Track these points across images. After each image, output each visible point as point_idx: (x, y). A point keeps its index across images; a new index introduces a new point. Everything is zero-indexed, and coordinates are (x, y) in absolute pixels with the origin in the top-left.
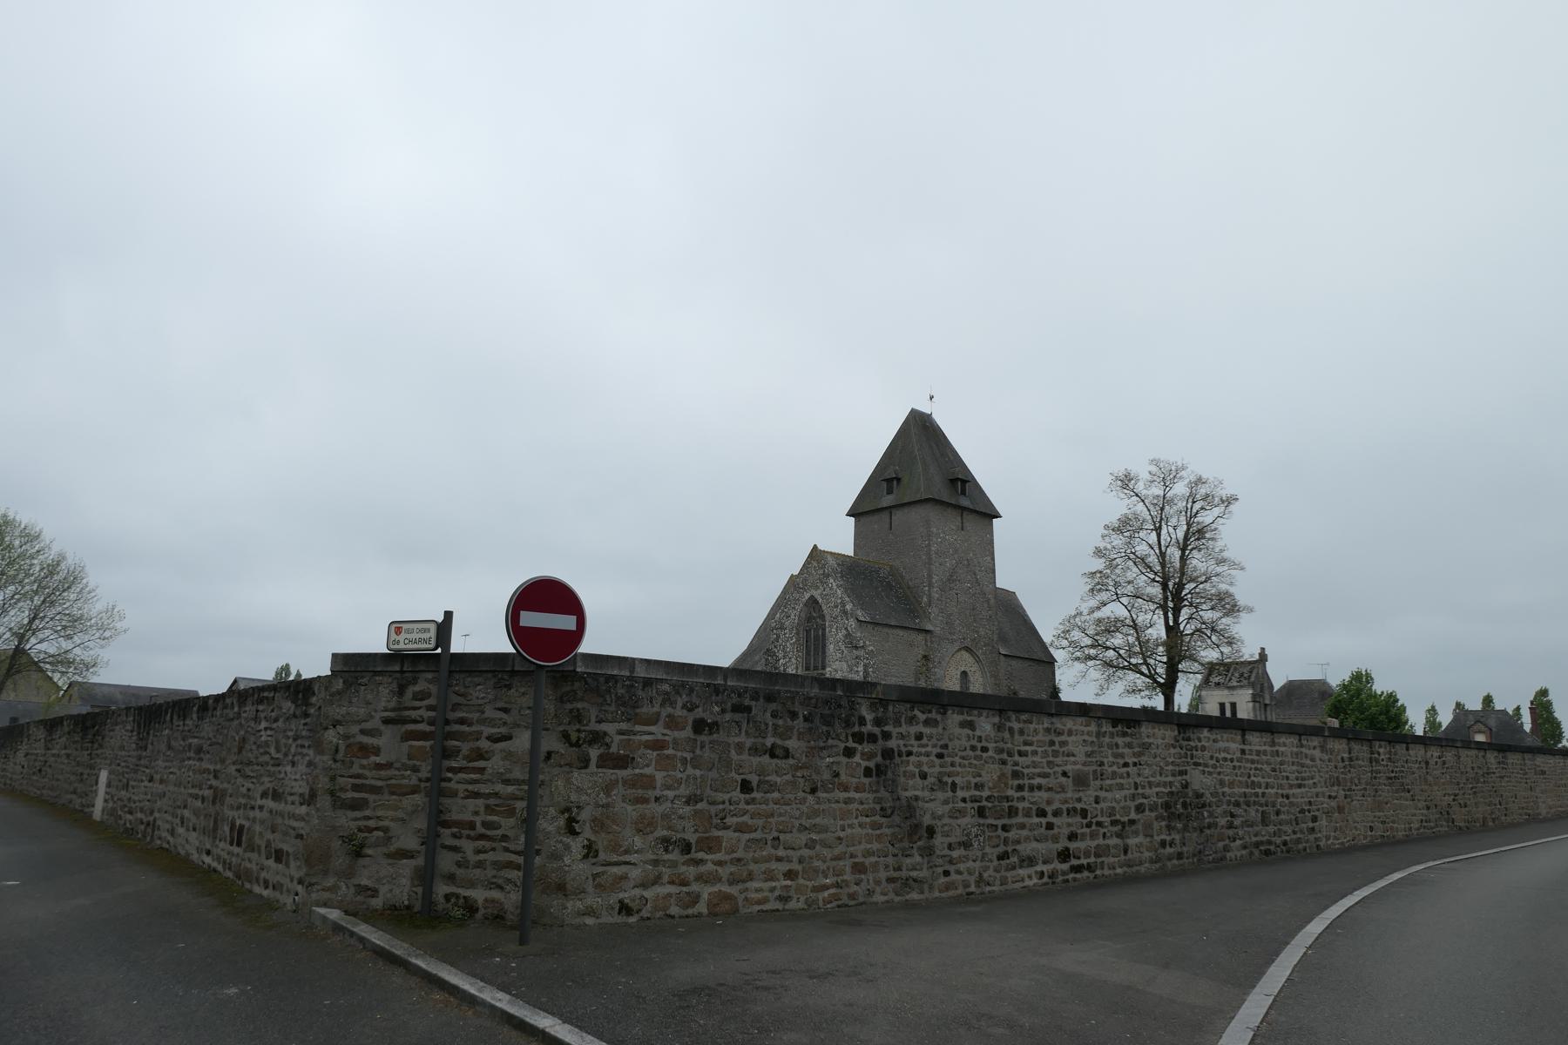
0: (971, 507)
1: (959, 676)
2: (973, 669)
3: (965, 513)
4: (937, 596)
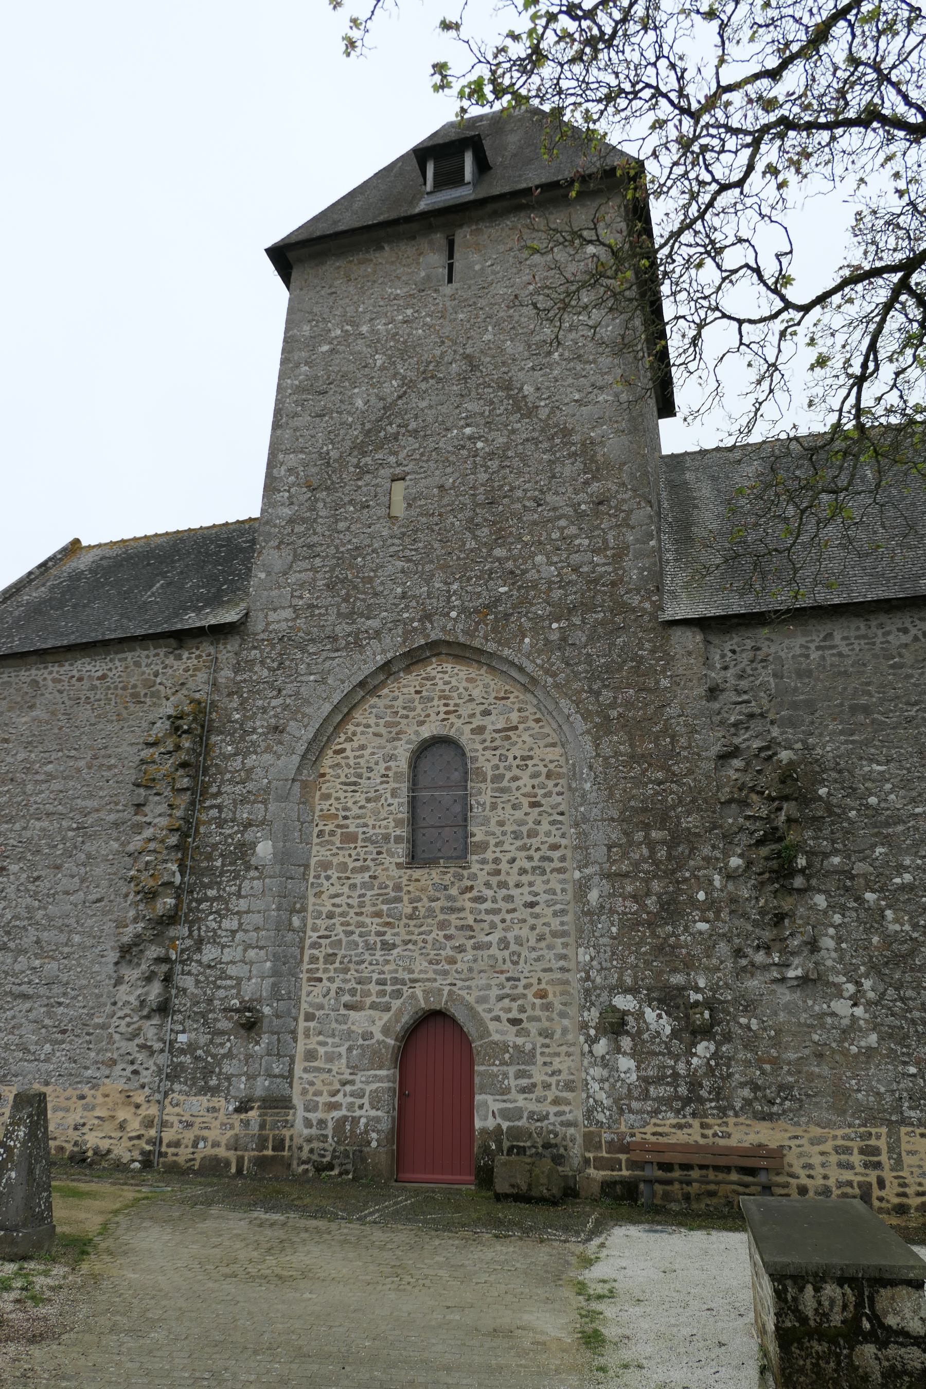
1: (402, 764)
2: (495, 722)
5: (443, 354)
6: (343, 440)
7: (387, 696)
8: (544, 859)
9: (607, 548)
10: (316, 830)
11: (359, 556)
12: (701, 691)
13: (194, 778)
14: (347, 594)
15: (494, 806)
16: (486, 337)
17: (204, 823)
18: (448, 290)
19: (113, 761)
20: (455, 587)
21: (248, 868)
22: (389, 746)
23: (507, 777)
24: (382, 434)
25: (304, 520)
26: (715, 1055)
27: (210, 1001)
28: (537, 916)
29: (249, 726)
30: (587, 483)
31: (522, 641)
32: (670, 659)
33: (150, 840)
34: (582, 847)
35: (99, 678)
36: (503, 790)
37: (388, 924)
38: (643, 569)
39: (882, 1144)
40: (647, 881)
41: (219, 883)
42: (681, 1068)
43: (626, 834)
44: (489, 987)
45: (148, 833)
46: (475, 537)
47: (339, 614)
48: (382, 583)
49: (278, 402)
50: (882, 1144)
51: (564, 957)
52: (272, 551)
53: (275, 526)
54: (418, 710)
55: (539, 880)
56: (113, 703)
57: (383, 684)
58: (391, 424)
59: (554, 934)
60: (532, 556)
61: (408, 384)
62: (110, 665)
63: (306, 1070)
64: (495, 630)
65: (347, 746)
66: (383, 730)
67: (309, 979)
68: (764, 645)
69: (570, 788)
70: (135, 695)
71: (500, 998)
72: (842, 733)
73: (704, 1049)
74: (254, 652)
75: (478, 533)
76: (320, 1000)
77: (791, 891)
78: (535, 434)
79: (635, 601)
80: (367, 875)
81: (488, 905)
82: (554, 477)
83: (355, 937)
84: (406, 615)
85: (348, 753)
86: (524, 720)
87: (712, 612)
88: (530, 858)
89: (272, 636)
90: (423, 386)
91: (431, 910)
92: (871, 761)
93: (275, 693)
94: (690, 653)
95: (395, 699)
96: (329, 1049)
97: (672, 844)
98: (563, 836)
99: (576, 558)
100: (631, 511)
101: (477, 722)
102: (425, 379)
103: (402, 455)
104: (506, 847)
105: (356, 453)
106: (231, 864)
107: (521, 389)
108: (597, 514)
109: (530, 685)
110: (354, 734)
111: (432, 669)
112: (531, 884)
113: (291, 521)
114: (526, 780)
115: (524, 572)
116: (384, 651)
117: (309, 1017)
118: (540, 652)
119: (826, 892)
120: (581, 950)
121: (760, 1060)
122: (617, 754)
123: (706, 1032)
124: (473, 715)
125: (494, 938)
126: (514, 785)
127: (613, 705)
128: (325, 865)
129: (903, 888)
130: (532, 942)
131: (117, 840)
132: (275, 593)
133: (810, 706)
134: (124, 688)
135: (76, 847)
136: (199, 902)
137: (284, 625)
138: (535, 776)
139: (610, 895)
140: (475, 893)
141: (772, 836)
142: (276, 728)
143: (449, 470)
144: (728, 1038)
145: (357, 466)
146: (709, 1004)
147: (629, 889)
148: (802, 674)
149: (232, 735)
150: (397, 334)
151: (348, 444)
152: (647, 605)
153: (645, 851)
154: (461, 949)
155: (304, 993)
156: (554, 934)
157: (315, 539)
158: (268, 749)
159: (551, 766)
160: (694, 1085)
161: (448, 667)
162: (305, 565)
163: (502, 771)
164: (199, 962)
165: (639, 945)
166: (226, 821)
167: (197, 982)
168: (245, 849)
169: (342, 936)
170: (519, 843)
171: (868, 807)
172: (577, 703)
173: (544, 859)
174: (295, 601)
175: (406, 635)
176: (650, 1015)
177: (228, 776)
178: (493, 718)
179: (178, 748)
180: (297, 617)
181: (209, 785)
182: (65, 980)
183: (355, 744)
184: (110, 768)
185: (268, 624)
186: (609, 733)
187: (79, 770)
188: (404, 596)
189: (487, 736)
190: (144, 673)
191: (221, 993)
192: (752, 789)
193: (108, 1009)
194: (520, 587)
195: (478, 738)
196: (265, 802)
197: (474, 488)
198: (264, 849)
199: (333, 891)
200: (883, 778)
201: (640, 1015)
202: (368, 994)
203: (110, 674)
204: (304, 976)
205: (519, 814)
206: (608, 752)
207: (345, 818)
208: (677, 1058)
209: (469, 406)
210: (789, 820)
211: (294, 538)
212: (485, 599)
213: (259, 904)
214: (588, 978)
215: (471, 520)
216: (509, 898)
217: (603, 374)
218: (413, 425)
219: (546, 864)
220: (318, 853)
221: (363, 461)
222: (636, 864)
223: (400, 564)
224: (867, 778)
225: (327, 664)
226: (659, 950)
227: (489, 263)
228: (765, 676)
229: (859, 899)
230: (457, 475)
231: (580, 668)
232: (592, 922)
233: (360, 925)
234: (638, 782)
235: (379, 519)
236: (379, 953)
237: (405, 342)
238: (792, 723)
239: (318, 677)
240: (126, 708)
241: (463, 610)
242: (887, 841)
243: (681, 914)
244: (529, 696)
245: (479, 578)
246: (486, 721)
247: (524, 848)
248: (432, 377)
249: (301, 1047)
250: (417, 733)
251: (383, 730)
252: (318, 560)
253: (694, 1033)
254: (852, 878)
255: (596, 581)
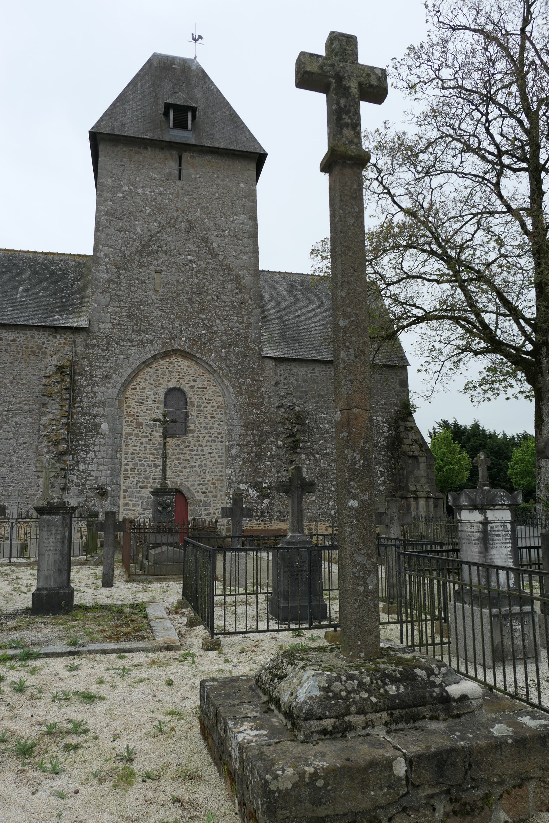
0: (193, 142)
1: (161, 397)
2: (199, 385)
3: (186, 156)
4: (106, 276)
5: (178, 216)
6: (132, 247)
7: (154, 368)
8: (215, 437)
9: (243, 323)
10: (125, 420)
11: (142, 305)
12: (273, 383)
13: (70, 394)
14: (137, 321)
15: (197, 417)
16: (197, 214)
17: (75, 414)
18: (179, 183)
19: (24, 382)
20: (184, 327)
21: (98, 433)
22: (155, 389)
23: (203, 405)
24: (150, 249)
25: (115, 283)
26: (269, 503)
27: (84, 485)
28: (212, 457)
29: (93, 373)
30: (237, 293)
31: (211, 355)
32: (264, 370)
33: (52, 420)
34: (230, 434)
35: (11, 341)
36: (201, 411)
37: (156, 458)
38: (256, 334)
39: (313, 527)
40: (252, 447)
41: (85, 439)
42: (259, 507)
43: (246, 431)
44: (195, 481)
45: (50, 416)
46: (192, 307)
47: (133, 330)
48: (152, 320)
49: (97, 217)
50: (313, 527)
51: (222, 471)
52: (99, 294)
53: (100, 282)
54: (167, 376)
55: (213, 444)
56: (21, 353)
57: (152, 363)
58: (154, 245)
59: (218, 464)
60: (215, 320)
61: (162, 227)
62: (18, 335)
63: (124, 510)
64: (200, 349)
65: (137, 387)
66: (153, 382)
67: (124, 477)
68: (294, 369)
69: (225, 412)
70: (33, 352)
71: (199, 485)
72: (315, 403)
73: (266, 501)
74: (94, 341)
75: (193, 305)
76: (129, 485)
77: (295, 453)
78: (218, 267)
79: (253, 346)
80: (147, 439)
81: (195, 452)
82: (224, 288)
83: (143, 462)
84: (163, 336)
85: (138, 390)
86: (209, 385)
87: (280, 355)
88: (210, 437)
89: (102, 335)
90: (169, 230)
91: (173, 454)
92: (322, 413)
93: (105, 361)
94: (270, 369)
95: (158, 370)
96: (134, 502)
97: (260, 436)
98: (222, 429)
99: (232, 324)
100: (252, 309)
101: (191, 383)
102: (170, 227)
103: (160, 261)
104: (202, 432)
105: (138, 255)
106: (90, 432)
107: (212, 244)
108: (241, 308)
109: (213, 372)
110: (140, 382)
111: (173, 359)
112: (210, 446)
113: (108, 281)
114: (209, 408)
115: (212, 326)
116: (154, 350)
117: (125, 491)
118: (217, 360)
119: (305, 454)
120: (228, 469)
121: (282, 504)
122: (244, 403)
123: (267, 496)
124: (190, 381)
125: (197, 464)
126: (205, 409)
127: (243, 384)
128: (130, 434)
129: (326, 454)
130: (211, 466)
131: (31, 417)
132: (102, 315)
133: (306, 392)
134: (27, 348)
135: (8, 419)
136: (76, 446)
137: (107, 331)
138: (213, 407)
139: (240, 452)
140: (190, 448)
141: (292, 435)
142: (106, 376)
143: (181, 274)
144: (274, 498)
145: (139, 261)
146: (269, 488)
147: (246, 450)
148: (305, 381)
149: (86, 377)
150: (156, 199)
151: (134, 249)
152: (257, 348)
153: (252, 437)
154: (185, 468)
155: (122, 482)
156: (218, 464)
157: (121, 293)
158: (103, 385)
159: (219, 404)
160: (263, 512)
161: (180, 360)
162: (116, 304)
163: (200, 403)
164: (78, 470)
165: (248, 468)
166: (86, 414)
167: (78, 478)
168: (95, 427)
169: (138, 461)
170: (207, 431)
171: (320, 428)
172: (231, 382)
173: (215, 437)
174: (112, 320)
175: (164, 344)
176: (250, 491)
177: (85, 394)
178: (197, 383)
179: (63, 380)
180: (114, 328)
181: (76, 397)
182: (11, 476)
183: (141, 387)
184: (23, 384)
185: (100, 329)
186: (242, 395)
187: (5, 384)
188: (162, 327)
189: (195, 389)
190: (37, 342)
191: (89, 482)
192: (287, 419)
193: (35, 488)
194: (210, 332)
195: (191, 390)
196: (103, 407)
197: (192, 285)
198: (104, 427)
199: (133, 444)
200: (325, 419)
201: (247, 491)
202: (149, 483)
203: (18, 340)
204: (122, 476)
205: (207, 420)
206: (241, 401)
207: (138, 416)
208: (258, 504)
209: (190, 246)
210: (298, 431)
211: (110, 290)
212: (196, 335)
213: (104, 448)
214: (230, 479)
215: (190, 299)
216: (202, 450)
217: (245, 247)
218: (165, 248)
219: (216, 439)
220: (126, 429)
221: (142, 260)
222: (249, 442)
223: (160, 312)
224: (320, 419)
225: (129, 351)
226: (254, 470)
227: (198, 176)
228: (293, 380)
229: (314, 456)
230: (184, 277)
231: (232, 369)
232: (232, 460)
233: (145, 458)
234: (251, 413)
235: (150, 289)
236: (153, 468)
237: (160, 204)
238: (300, 398)
239: (125, 357)
240: (29, 357)
241: (187, 338)
242: (324, 439)
243: (262, 459)
244: (211, 376)
245: (194, 325)
246: (195, 384)
247: (208, 433)
248: (173, 227)
249: (122, 502)
250: (167, 385)
251: (153, 382)
252: (122, 303)
253: (264, 496)
254: (313, 450)
255: (239, 335)
